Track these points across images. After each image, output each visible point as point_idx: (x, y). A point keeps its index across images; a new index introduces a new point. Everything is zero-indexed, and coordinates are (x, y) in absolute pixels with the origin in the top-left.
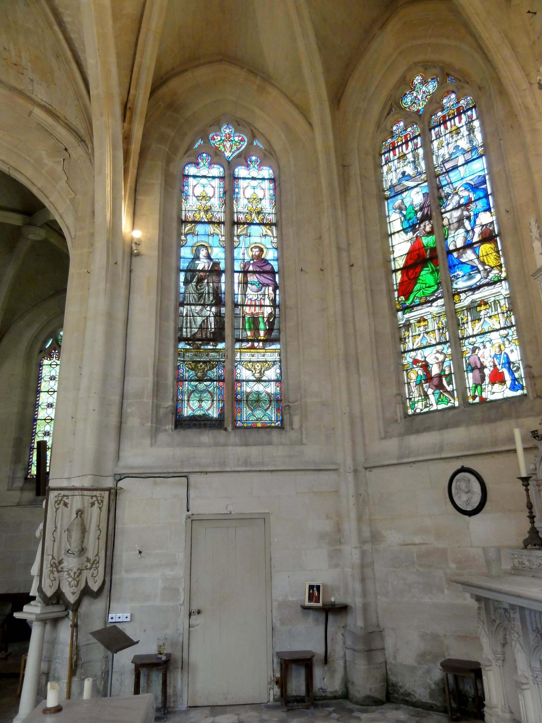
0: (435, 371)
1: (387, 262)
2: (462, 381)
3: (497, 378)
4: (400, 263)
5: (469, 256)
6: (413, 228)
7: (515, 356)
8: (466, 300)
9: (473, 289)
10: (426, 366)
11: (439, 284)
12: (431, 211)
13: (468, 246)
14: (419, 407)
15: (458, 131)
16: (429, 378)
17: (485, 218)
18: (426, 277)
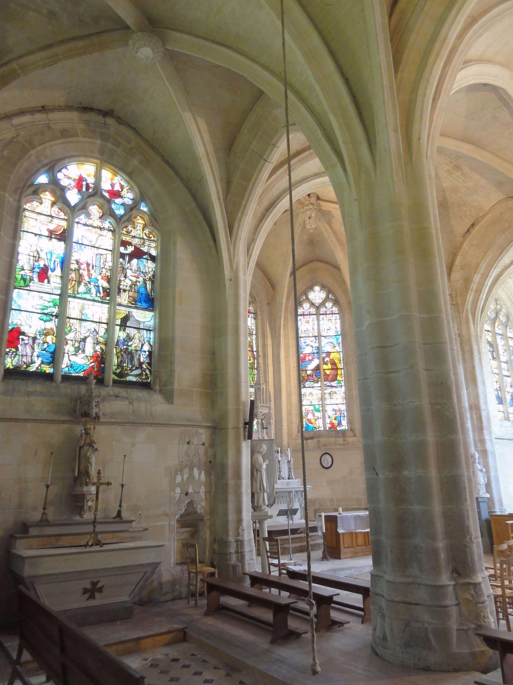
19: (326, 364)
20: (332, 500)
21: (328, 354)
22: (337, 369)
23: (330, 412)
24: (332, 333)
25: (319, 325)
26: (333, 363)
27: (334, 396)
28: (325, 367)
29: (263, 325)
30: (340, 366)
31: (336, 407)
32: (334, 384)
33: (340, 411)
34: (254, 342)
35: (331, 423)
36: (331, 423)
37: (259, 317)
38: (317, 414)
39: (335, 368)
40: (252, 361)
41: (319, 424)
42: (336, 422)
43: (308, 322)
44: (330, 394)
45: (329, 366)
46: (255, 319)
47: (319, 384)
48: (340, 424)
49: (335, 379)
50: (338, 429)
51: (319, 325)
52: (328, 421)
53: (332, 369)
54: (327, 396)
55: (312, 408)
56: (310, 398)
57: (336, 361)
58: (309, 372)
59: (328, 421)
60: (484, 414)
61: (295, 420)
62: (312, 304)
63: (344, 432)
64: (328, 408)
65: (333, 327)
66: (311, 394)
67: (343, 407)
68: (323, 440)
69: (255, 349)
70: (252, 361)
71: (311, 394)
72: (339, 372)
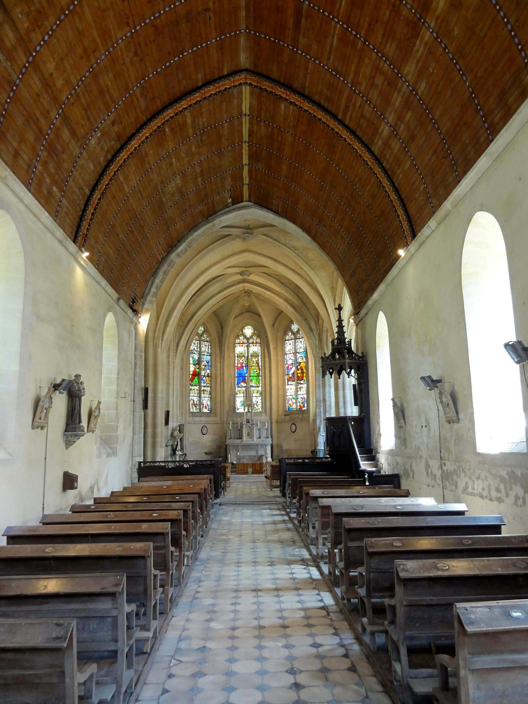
0: (195, 403)
1: (190, 371)
2: (200, 407)
3: (206, 408)
4: (191, 373)
5: (204, 378)
6: (194, 365)
7: (209, 404)
8: (203, 388)
9: (205, 387)
10: (194, 401)
11: (199, 382)
12: (198, 363)
13: (205, 376)
14: (191, 410)
15: (206, 346)
16: (194, 404)
17: (208, 371)
18: (196, 379)
19: (298, 370)
20: (295, 450)
21: (300, 363)
22: (304, 373)
23: (300, 400)
24: (302, 350)
25: (295, 346)
26: (302, 369)
27: (302, 390)
28: (298, 372)
29: (264, 349)
30: (305, 371)
31: (302, 396)
32: (302, 382)
33: (304, 398)
34: (260, 360)
35: (300, 406)
36: (300, 406)
37: (262, 345)
38: (294, 401)
39: (302, 373)
40: (258, 371)
41: (294, 406)
42: (302, 405)
43: (290, 344)
44: (300, 388)
45: (300, 371)
46: (261, 346)
47: (294, 383)
48: (304, 406)
49: (302, 379)
50: (303, 409)
51: (295, 346)
52: (298, 404)
53: (301, 373)
54: (299, 390)
55: (291, 397)
56: (290, 391)
57: (304, 368)
58: (290, 376)
59: (298, 404)
60: (327, 403)
61: (281, 404)
62: (293, 333)
63: (305, 410)
64: (299, 397)
65: (302, 346)
66: (291, 389)
67: (305, 396)
68: (293, 416)
69: (260, 365)
70: (258, 371)
71: (291, 389)
72: (305, 375)
